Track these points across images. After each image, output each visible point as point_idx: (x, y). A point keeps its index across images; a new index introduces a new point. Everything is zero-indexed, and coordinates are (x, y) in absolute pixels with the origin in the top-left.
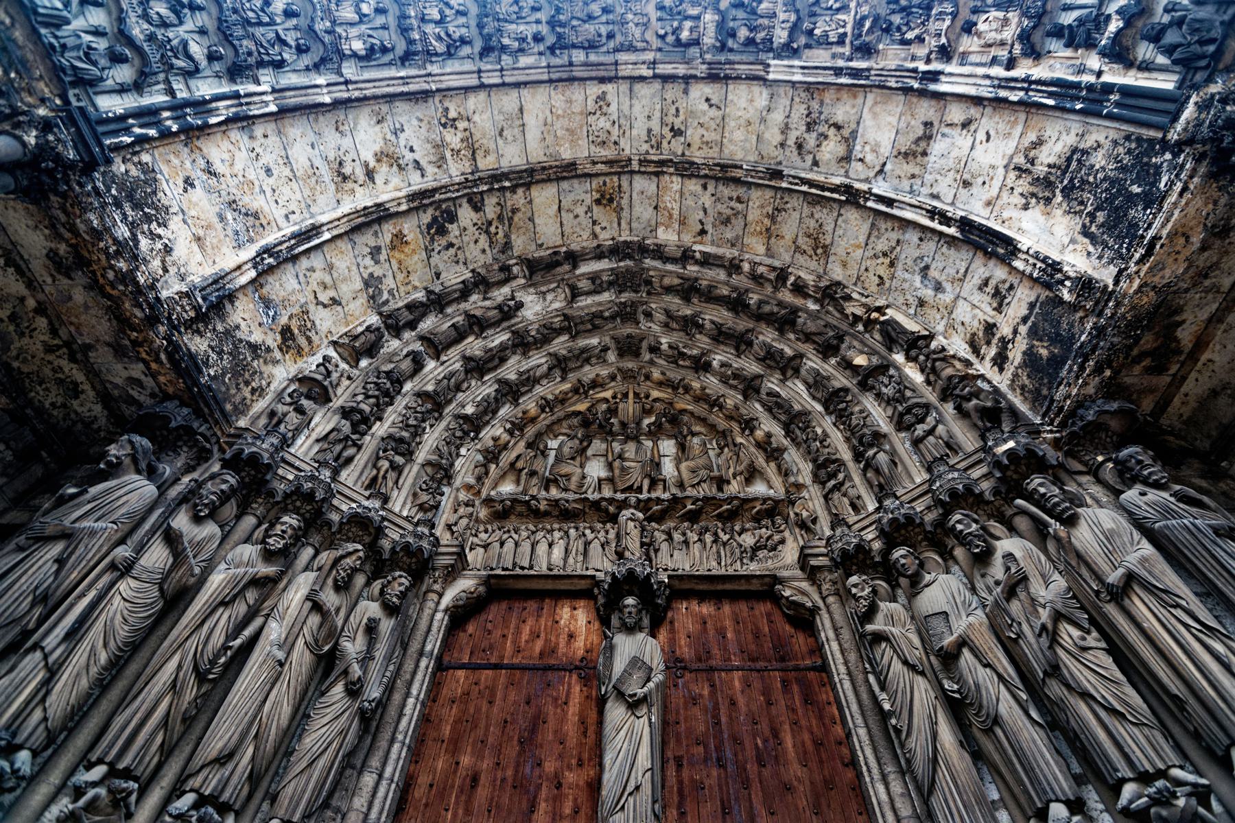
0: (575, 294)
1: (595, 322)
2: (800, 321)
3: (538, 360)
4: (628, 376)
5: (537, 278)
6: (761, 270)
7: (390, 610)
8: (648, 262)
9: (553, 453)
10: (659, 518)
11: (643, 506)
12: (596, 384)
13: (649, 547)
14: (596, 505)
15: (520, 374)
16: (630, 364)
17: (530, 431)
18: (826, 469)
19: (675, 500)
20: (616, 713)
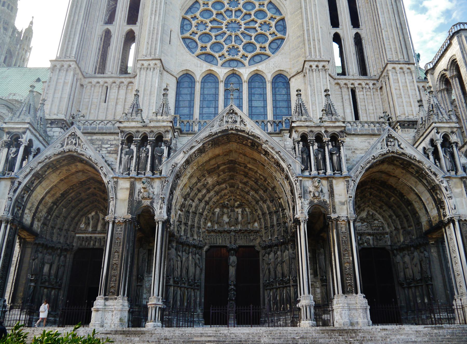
0: (219, 175)
1: (224, 181)
2: (267, 192)
3: (212, 193)
4: (232, 192)
5: (211, 173)
6: (261, 177)
7: (199, 255)
8: (236, 165)
9: (217, 213)
10: (237, 233)
11: (235, 231)
12: (225, 195)
13: (235, 241)
14: (226, 231)
15: (209, 198)
16: (232, 189)
17: (212, 210)
18: (266, 227)
19: (240, 230)
20: (230, 267)
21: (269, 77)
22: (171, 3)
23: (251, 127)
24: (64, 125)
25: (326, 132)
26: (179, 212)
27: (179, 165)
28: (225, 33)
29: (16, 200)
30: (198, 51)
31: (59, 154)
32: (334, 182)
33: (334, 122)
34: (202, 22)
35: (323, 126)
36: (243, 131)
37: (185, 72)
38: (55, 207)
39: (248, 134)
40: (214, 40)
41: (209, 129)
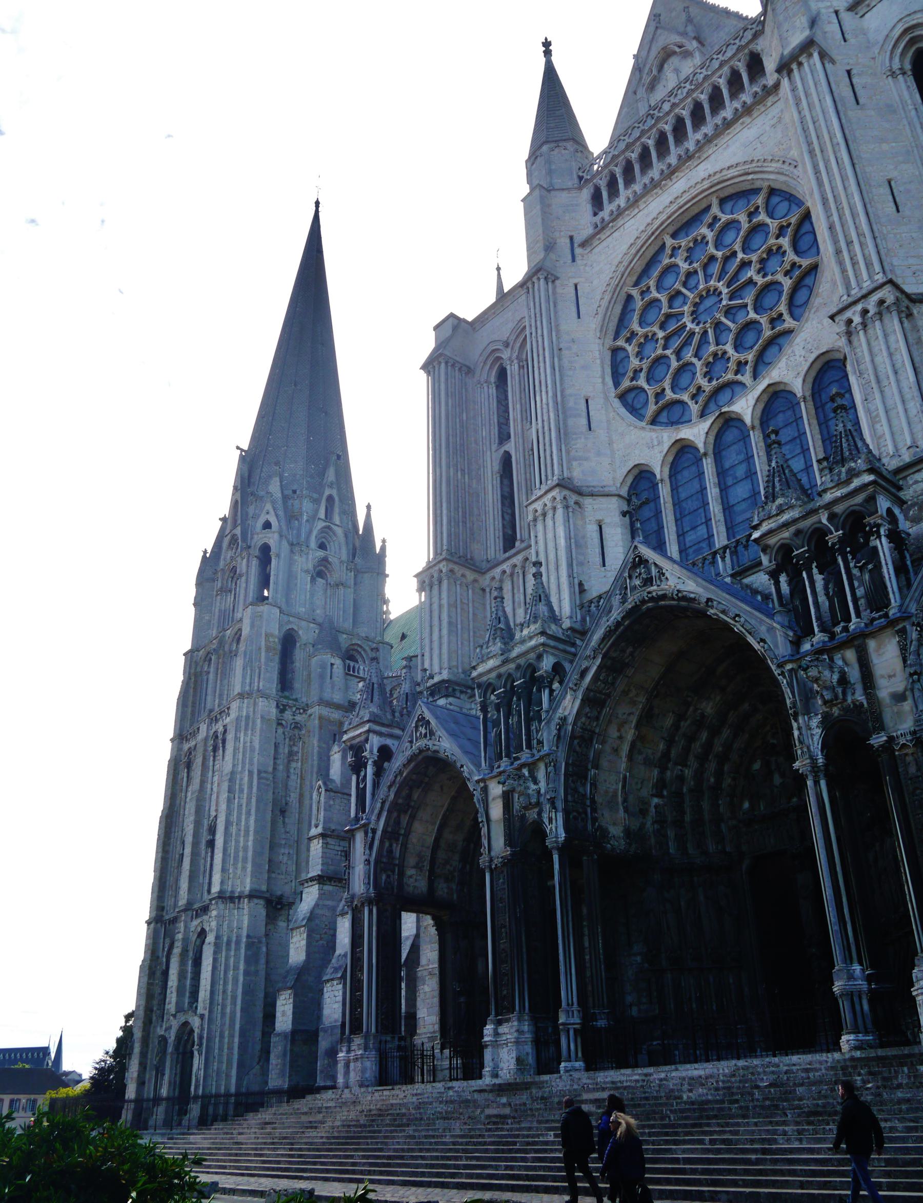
3: (726, 733)
21: (798, 387)
22: (573, 341)
23: (678, 580)
24: (450, 689)
25: (832, 517)
26: (656, 800)
27: (571, 719)
28: (694, 333)
29: (377, 862)
30: (652, 408)
31: (410, 761)
32: (872, 644)
33: (848, 482)
34: (646, 337)
35: (820, 507)
36: (664, 597)
37: (636, 472)
38: (472, 846)
39: (673, 599)
40: (674, 364)
41: (605, 619)
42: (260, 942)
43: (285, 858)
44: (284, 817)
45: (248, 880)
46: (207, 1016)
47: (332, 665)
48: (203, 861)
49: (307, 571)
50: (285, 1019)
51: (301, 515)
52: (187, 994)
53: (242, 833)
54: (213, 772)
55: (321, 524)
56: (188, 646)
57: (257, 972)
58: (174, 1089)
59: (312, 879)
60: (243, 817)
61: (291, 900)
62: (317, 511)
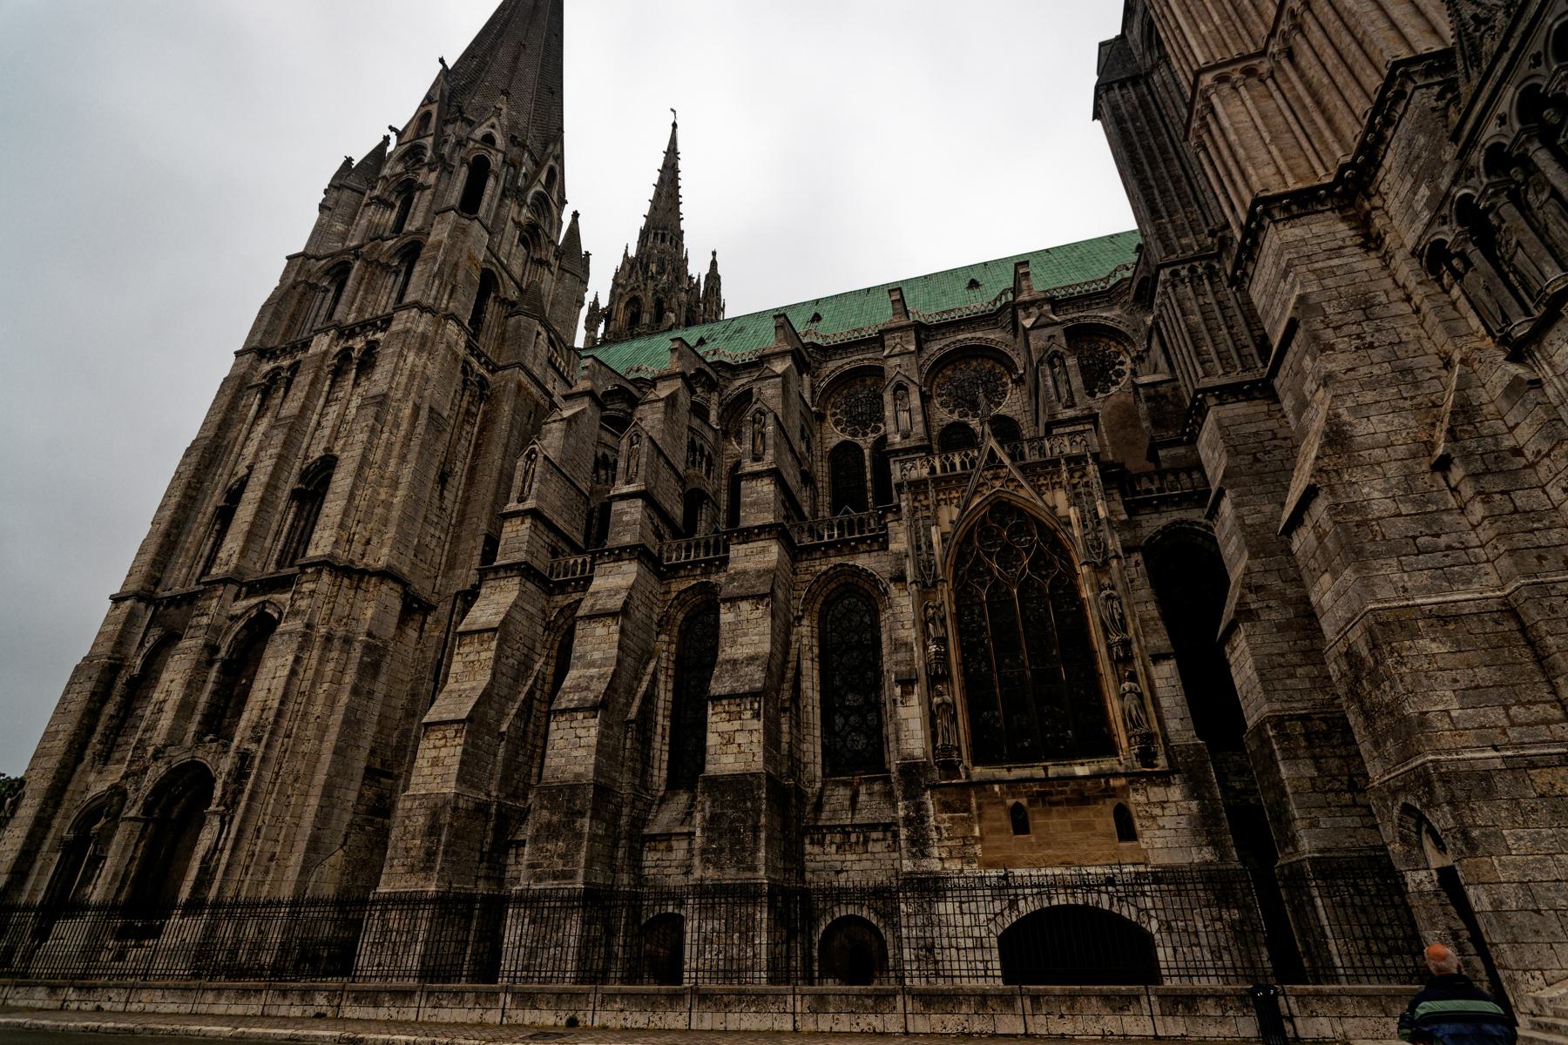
42: (385, 648)
43: (434, 542)
44: (443, 488)
45: (385, 551)
46: (260, 754)
47: (539, 334)
48: (278, 517)
49: (517, 224)
50: (438, 770)
51: (521, 164)
52: (197, 717)
53: (386, 482)
54: (327, 401)
55: (539, 188)
56: (300, 248)
57: (370, 694)
58: (120, 890)
59: (508, 568)
60: (393, 462)
61: (434, 599)
62: (537, 173)
